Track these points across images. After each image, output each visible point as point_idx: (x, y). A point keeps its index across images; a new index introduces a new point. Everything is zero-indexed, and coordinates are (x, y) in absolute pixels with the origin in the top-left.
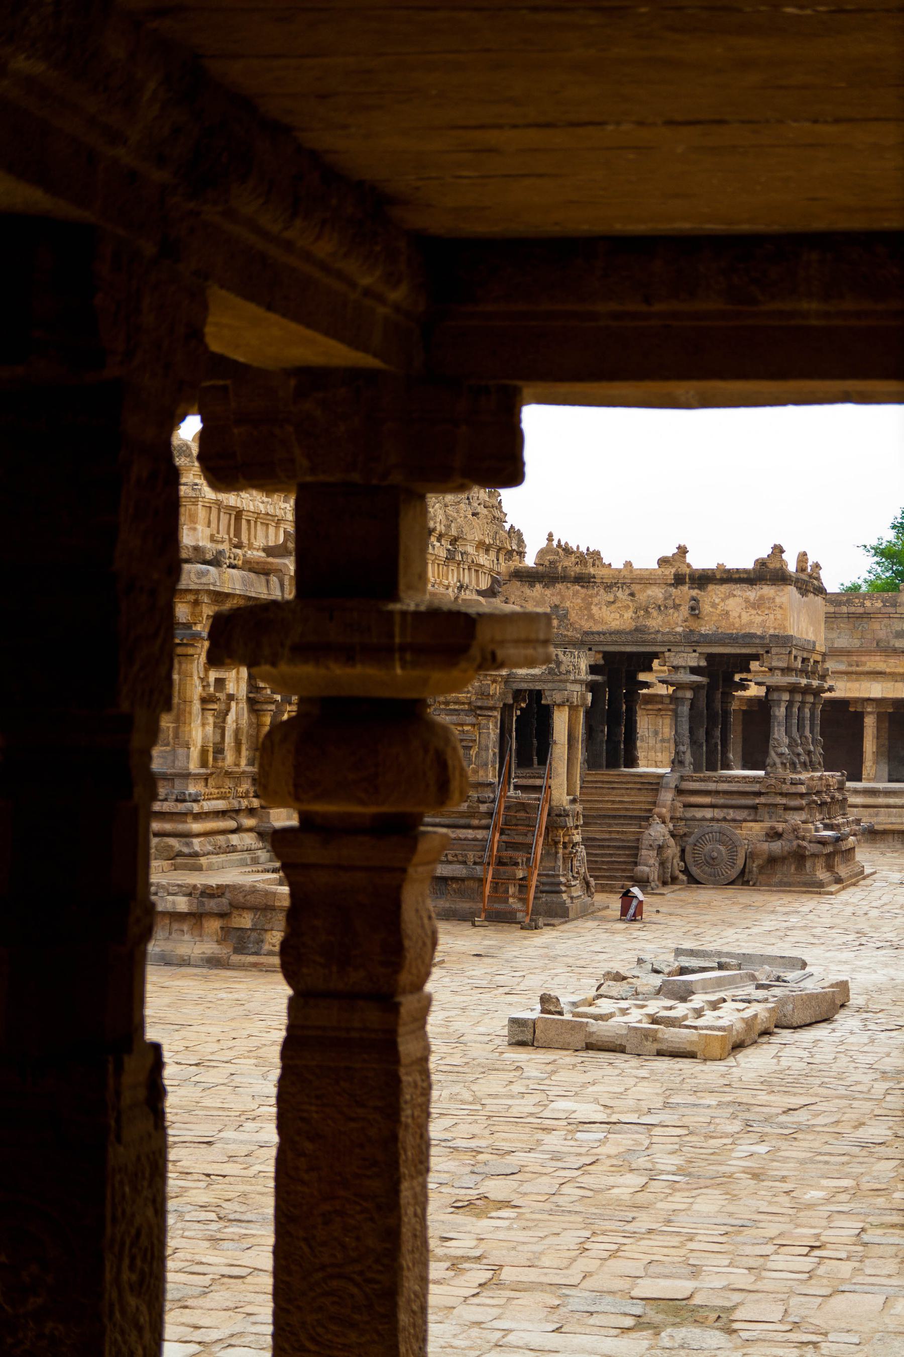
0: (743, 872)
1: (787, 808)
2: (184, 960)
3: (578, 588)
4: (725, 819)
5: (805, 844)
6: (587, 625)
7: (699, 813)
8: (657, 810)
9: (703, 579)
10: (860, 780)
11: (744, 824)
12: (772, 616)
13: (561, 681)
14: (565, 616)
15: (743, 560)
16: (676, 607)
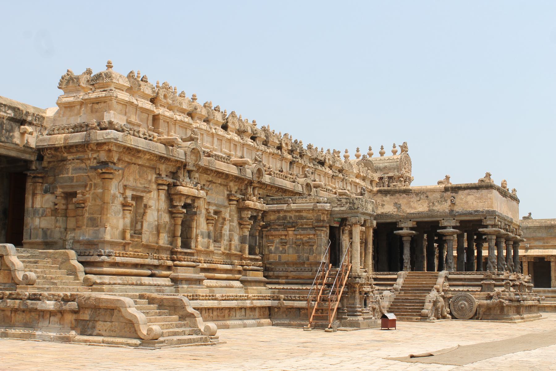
0: (476, 314)
1: (496, 286)
2: (51, 338)
3: (404, 195)
4: (468, 291)
5: (503, 301)
6: (409, 211)
7: (457, 289)
8: (435, 286)
9: (456, 189)
10: (550, 287)
11: (477, 293)
12: (486, 203)
13: (355, 213)
14: (400, 207)
15: (475, 181)
16: (446, 201)
